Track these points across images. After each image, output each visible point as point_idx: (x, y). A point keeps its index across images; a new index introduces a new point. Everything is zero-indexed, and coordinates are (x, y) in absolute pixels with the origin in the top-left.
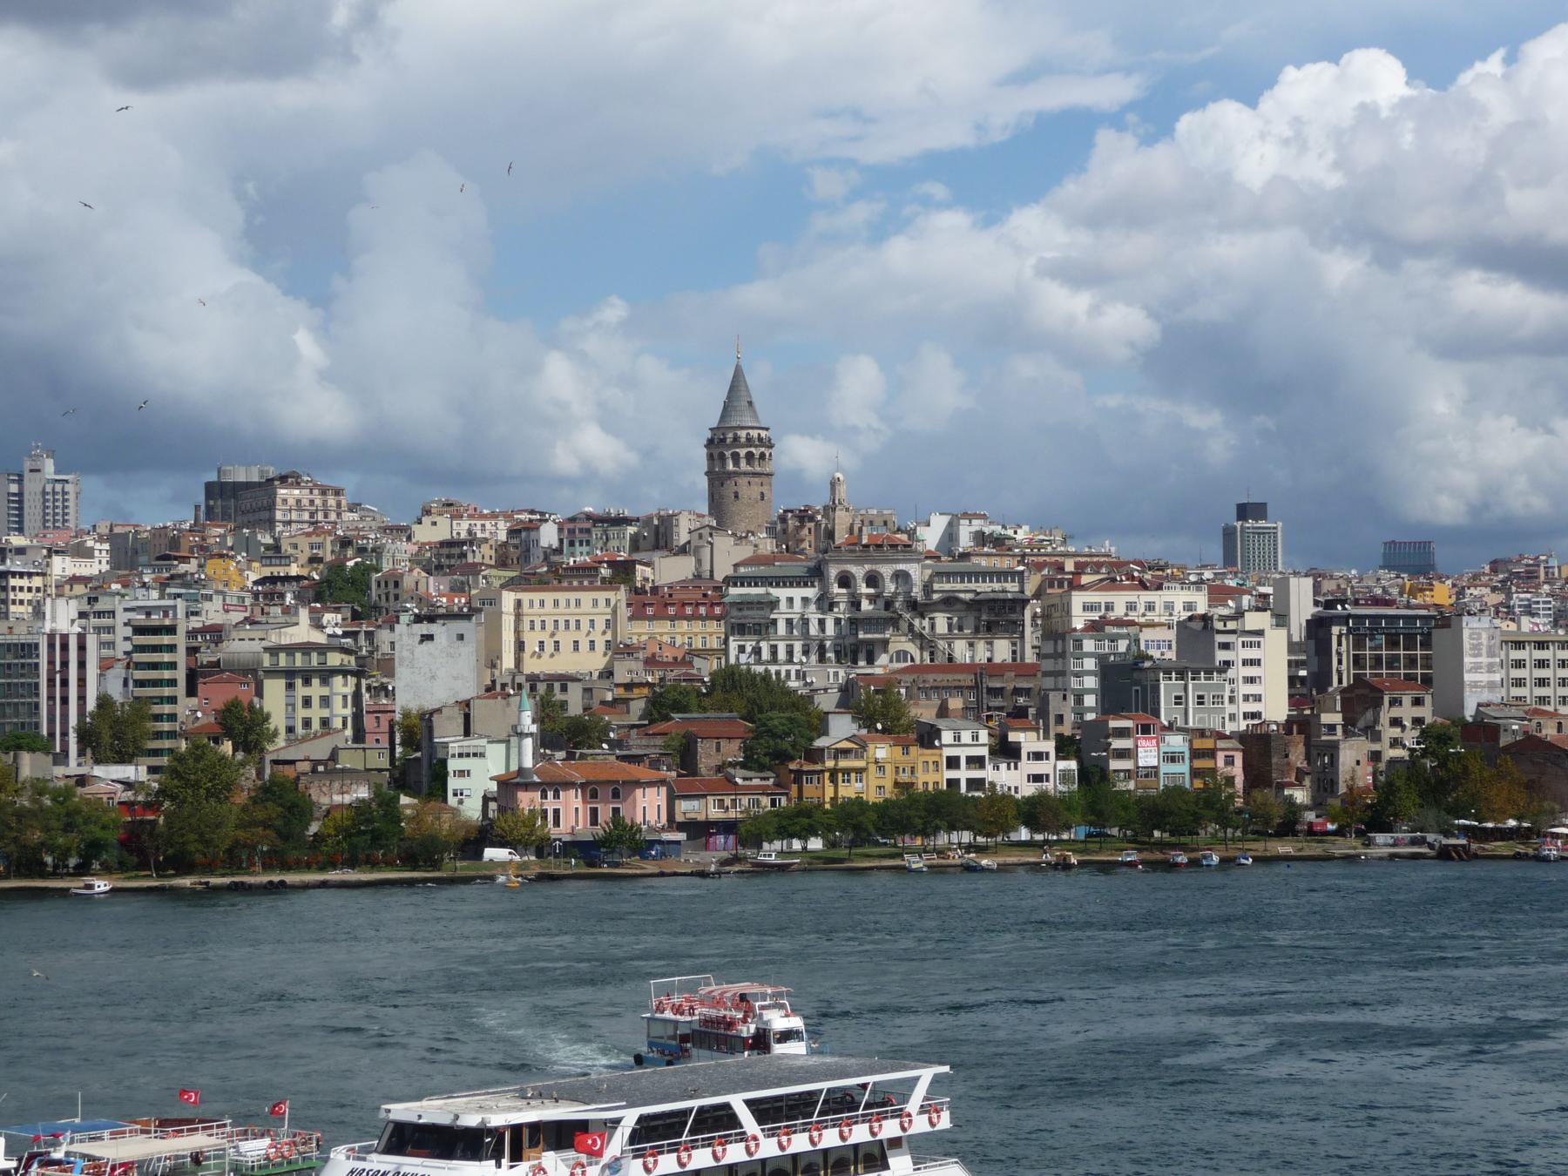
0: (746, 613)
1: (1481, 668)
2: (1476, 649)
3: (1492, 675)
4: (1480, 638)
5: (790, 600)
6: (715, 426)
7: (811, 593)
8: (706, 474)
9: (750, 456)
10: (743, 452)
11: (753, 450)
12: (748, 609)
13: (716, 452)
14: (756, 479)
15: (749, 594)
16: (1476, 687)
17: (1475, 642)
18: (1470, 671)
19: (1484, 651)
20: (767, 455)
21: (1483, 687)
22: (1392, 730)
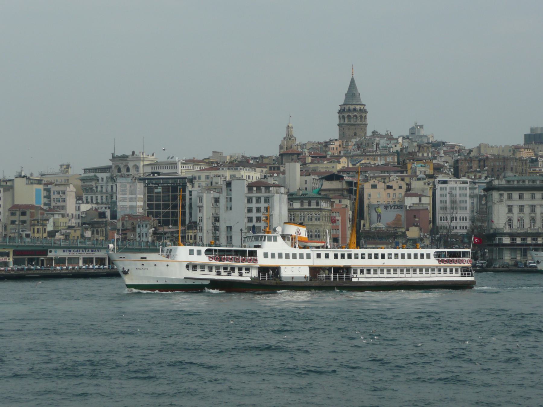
0: (86, 183)
1: (126, 200)
2: (124, 192)
3: (131, 202)
4: (126, 187)
5: (102, 179)
6: (342, 104)
7: (108, 175)
8: (338, 125)
9: (349, 116)
10: (346, 115)
11: (351, 115)
12: (87, 182)
13: (341, 116)
14: (352, 127)
15: (89, 176)
16: (124, 208)
17: (123, 188)
18: (121, 201)
19: (128, 191)
20: (358, 115)
21: (125, 208)
22: (11, 225)
